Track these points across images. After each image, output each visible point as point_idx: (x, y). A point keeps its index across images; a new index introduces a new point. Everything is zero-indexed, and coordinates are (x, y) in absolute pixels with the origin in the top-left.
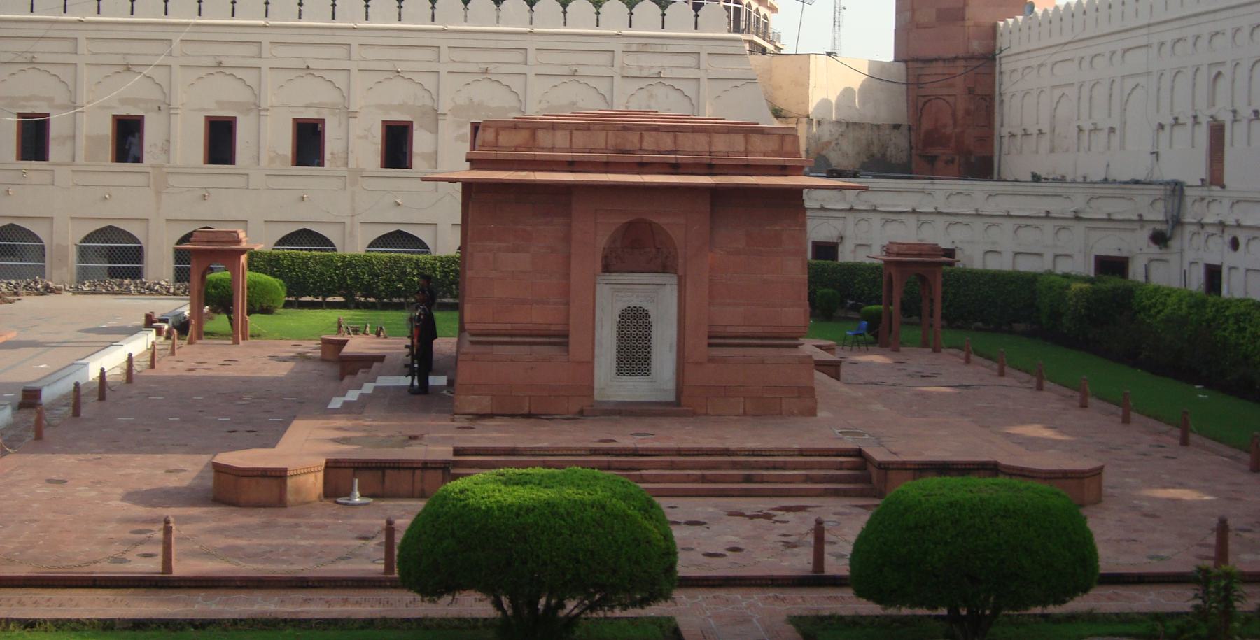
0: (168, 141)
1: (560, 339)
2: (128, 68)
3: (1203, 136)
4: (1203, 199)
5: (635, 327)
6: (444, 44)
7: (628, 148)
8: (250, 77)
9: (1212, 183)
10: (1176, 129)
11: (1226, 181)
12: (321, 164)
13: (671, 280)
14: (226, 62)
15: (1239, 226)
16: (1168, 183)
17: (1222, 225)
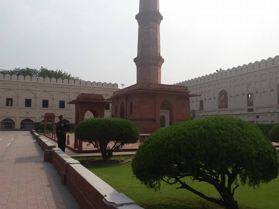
0: (18, 103)
1: (154, 120)
2: (10, 89)
3: (198, 103)
4: (199, 112)
5: (163, 118)
6: (71, 88)
7: (163, 88)
8: (34, 92)
9: (201, 110)
10: (193, 103)
11: (204, 109)
12: (48, 107)
13: (168, 111)
14: (30, 89)
15: (207, 115)
16: (192, 110)
17: (204, 116)
